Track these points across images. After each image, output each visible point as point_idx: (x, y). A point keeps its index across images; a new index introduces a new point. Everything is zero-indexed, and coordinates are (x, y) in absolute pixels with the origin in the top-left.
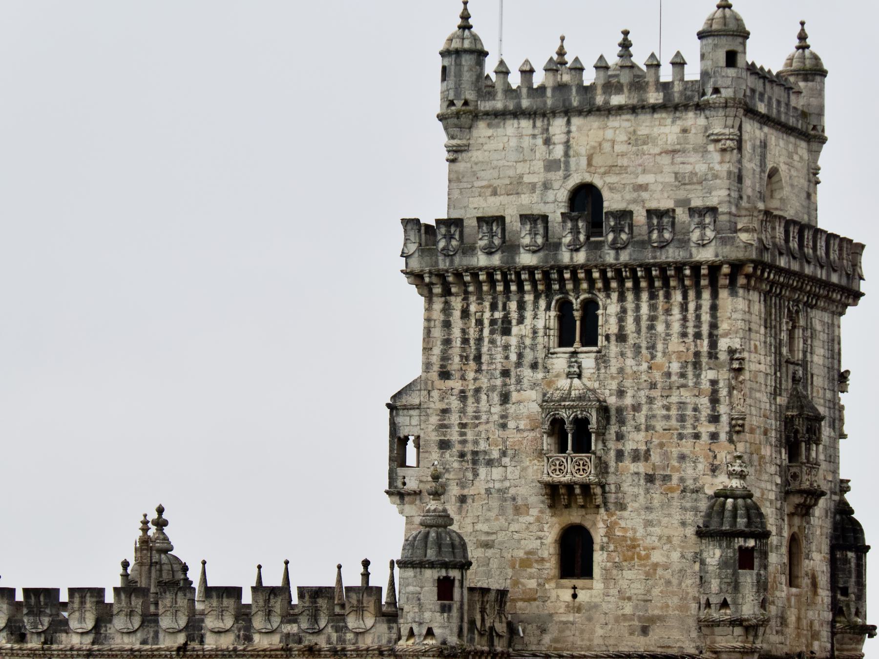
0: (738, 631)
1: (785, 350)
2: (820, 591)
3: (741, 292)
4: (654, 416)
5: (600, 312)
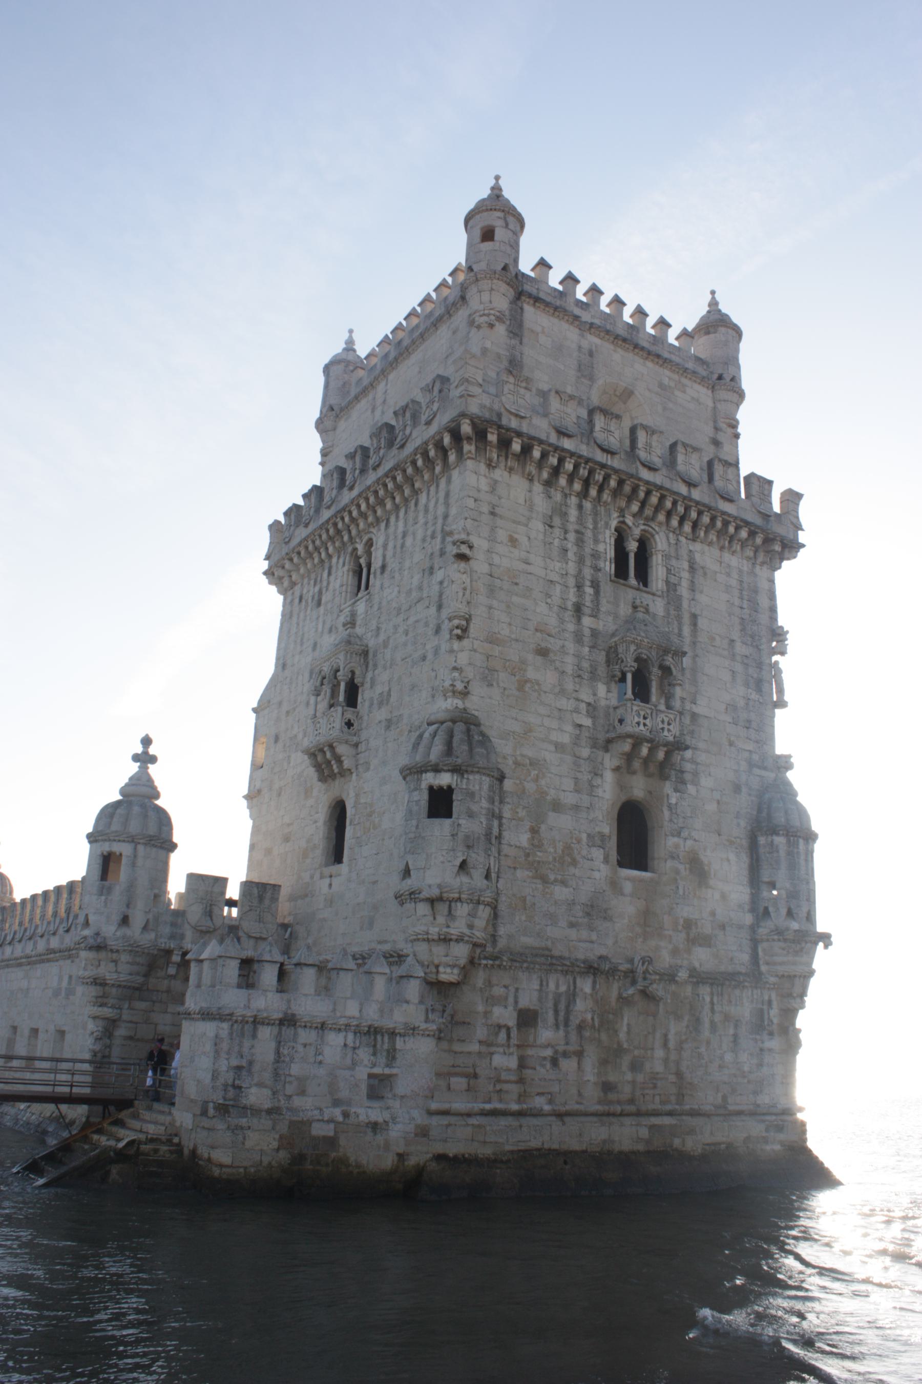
0: (423, 909)
1: (609, 567)
2: (712, 882)
3: (469, 463)
4: (396, 647)
5: (373, 549)
